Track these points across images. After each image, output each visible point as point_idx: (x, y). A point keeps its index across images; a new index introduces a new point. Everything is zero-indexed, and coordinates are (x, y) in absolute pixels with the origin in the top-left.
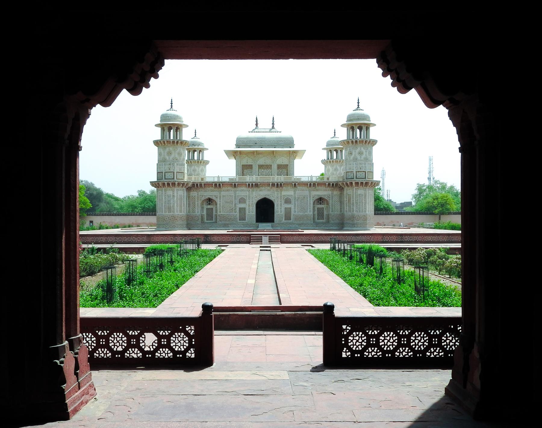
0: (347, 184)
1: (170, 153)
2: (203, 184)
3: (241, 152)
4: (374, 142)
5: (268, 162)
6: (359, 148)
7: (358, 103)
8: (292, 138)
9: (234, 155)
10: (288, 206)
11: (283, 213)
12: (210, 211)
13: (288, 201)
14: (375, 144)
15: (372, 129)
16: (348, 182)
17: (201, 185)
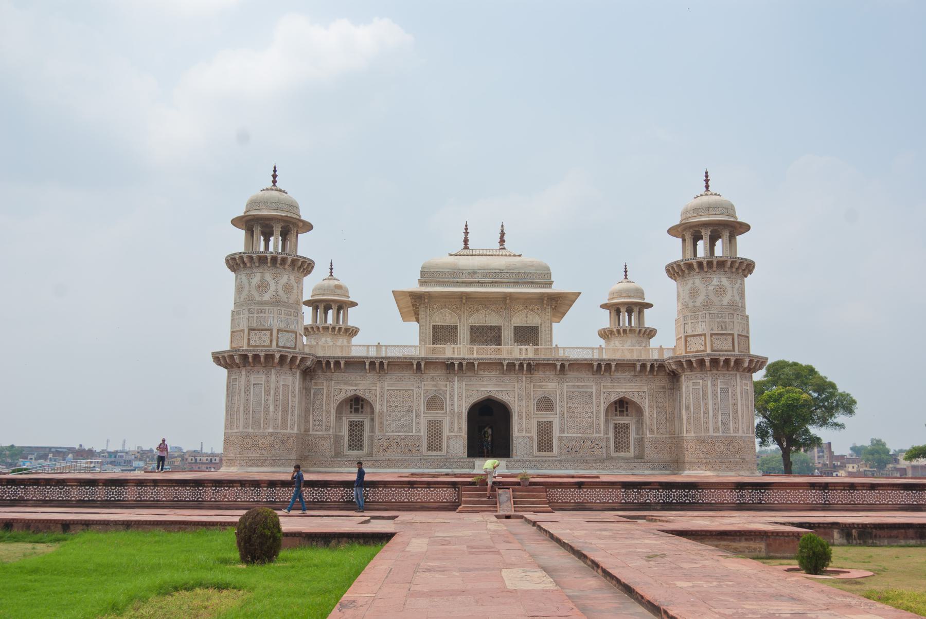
0: (690, 362)
1: (262, 287)
2: (342, 362)
3: (429, 295)
4: (747, 267)
5: (492, 319)
6: (715, 281)
7: (707, 181)
8: (548, 269)
9: (413, 305)
10: (546, 416)
11: (534, 434)
12: (356, 429)
13: (545, 404)
14: (750, 272)
15: (740, 239)
16: (693, 360)
17: (337, 363)
